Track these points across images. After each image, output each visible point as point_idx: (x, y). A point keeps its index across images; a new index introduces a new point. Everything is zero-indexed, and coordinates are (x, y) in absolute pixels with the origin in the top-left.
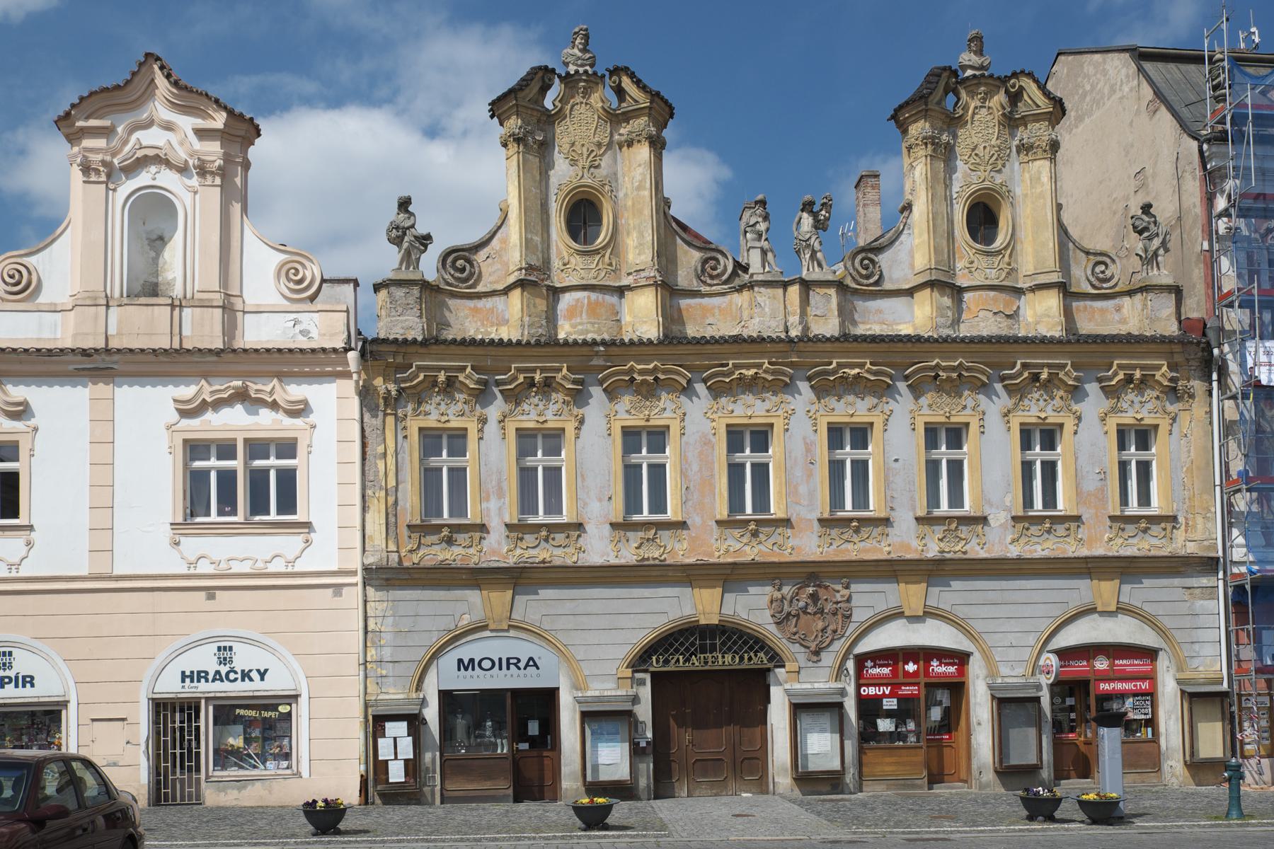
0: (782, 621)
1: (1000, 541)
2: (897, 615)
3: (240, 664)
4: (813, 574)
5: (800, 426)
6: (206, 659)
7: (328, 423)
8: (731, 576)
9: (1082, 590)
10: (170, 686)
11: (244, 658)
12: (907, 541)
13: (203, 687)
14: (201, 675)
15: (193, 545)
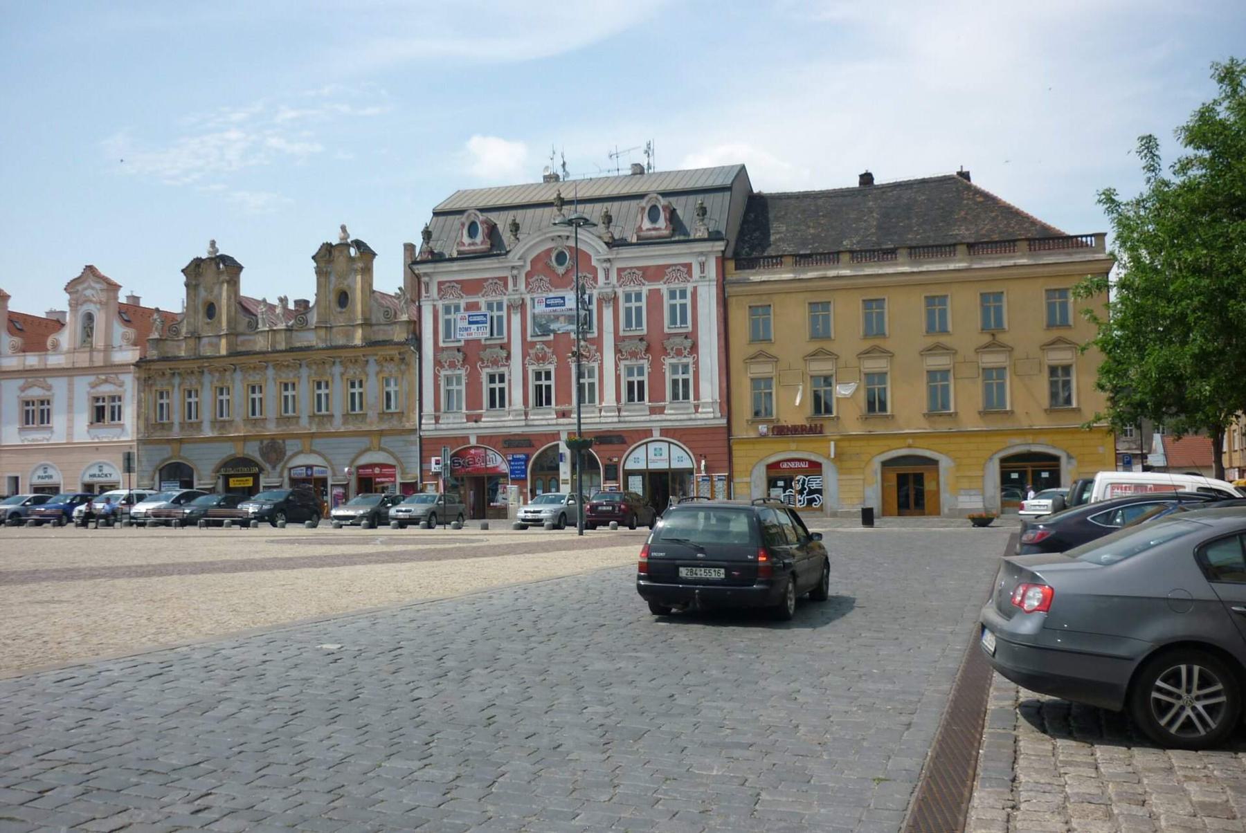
0: (263, 454)
1: (337, 425)
2: (301, 452)
3: (105, 471)
4: (273, 439)
5: (271, 383)
6: (95, 471)
7: (129, 386)
8: (245, 439)
9: (364, 442)
10: (87, 479)
11: (106, 470)
12: (305, 426)
13: (95, 479)
14: (94, 476)
15: (95, 431)
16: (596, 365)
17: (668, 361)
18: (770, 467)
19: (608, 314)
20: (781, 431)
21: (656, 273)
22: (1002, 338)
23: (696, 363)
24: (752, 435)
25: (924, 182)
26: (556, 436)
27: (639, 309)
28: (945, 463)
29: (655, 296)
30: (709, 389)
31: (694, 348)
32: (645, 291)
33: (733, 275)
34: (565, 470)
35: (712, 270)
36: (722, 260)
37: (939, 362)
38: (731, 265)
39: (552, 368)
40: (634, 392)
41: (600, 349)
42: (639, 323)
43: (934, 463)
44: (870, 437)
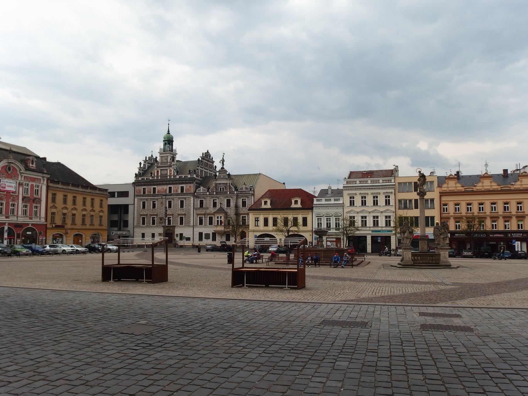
16: (16, 203)
17: (34, 205)
18: (53, 235)
19: (21, 188)
20: (57, 227)
21: (33, 180)
22: (94, 209)
23: (40, 206)
24: (51, 227)
25: (70, 169)
26: (4, 224)
27: (27, 189)
28: (84, 236)
29: (32, 185)
30: (43, 214)
31: (40, 203)
32: (30, 183)
33: (51, 185)
34: (6, 235)
35: (45, 182)
36: (48, 179)
37: (84, 213)
38: (49, 181)
39: (4, 202)
40: (25, 212)
41: (18, 199)
42: (27, 193)
43: (81, 235)
44: (72, 229)
